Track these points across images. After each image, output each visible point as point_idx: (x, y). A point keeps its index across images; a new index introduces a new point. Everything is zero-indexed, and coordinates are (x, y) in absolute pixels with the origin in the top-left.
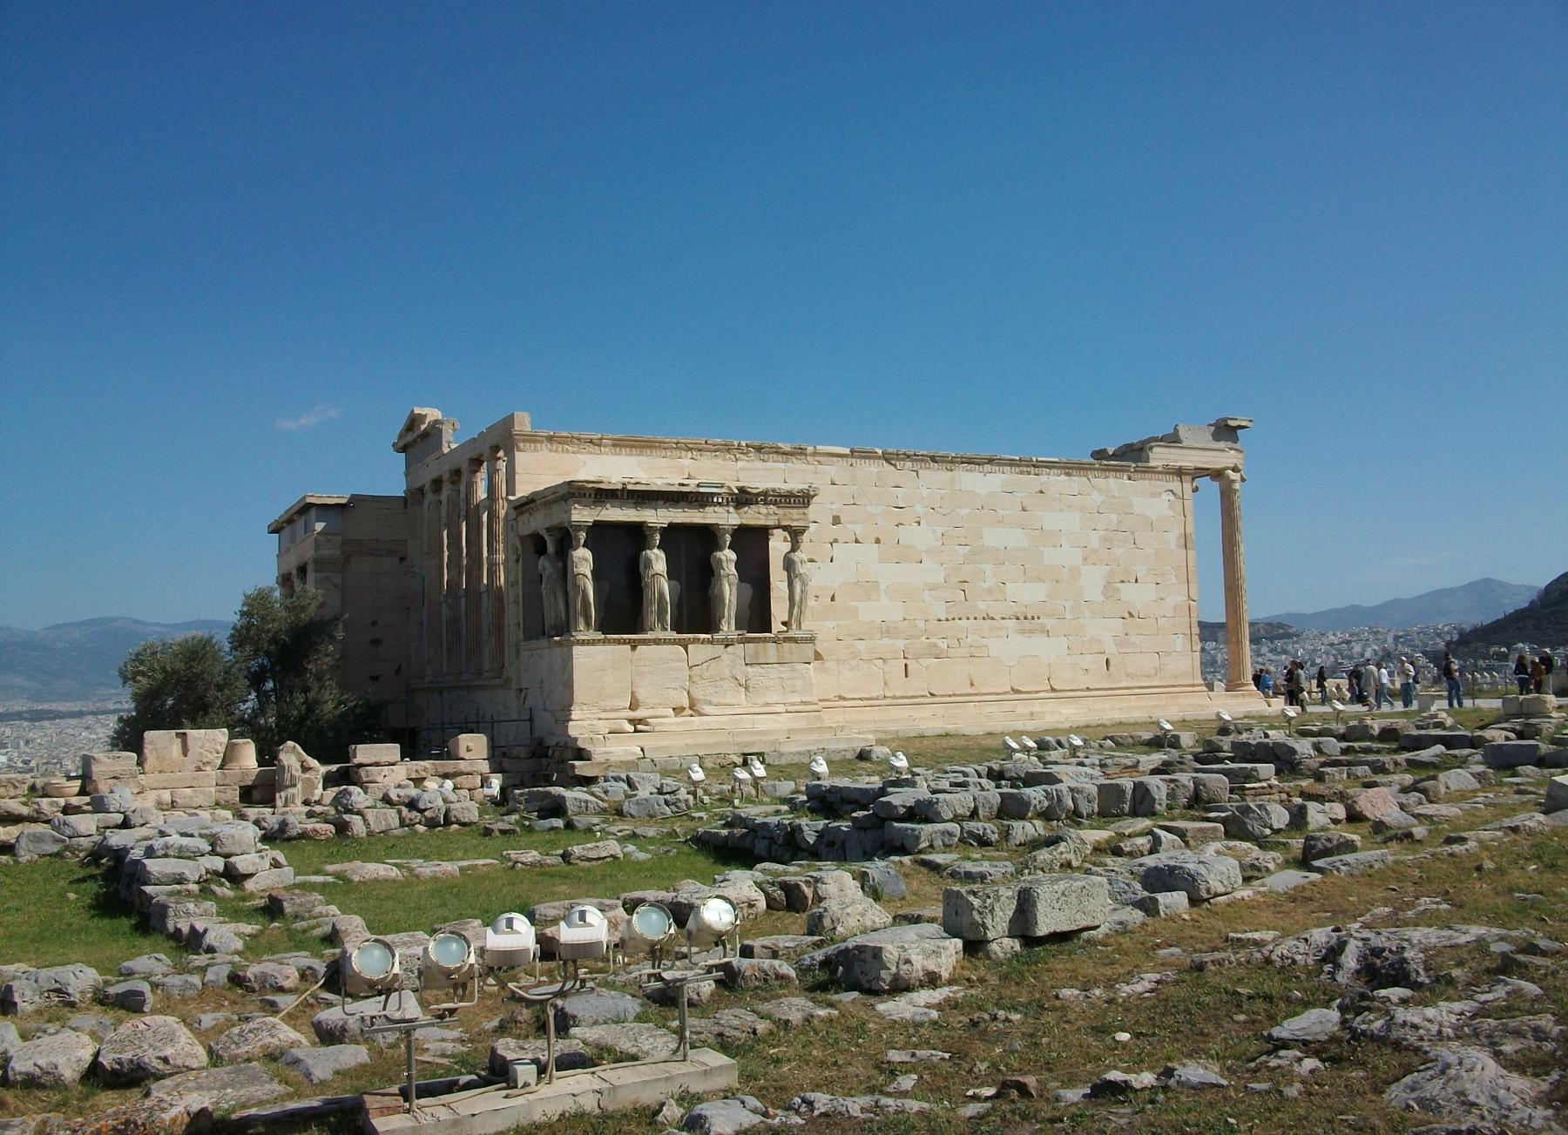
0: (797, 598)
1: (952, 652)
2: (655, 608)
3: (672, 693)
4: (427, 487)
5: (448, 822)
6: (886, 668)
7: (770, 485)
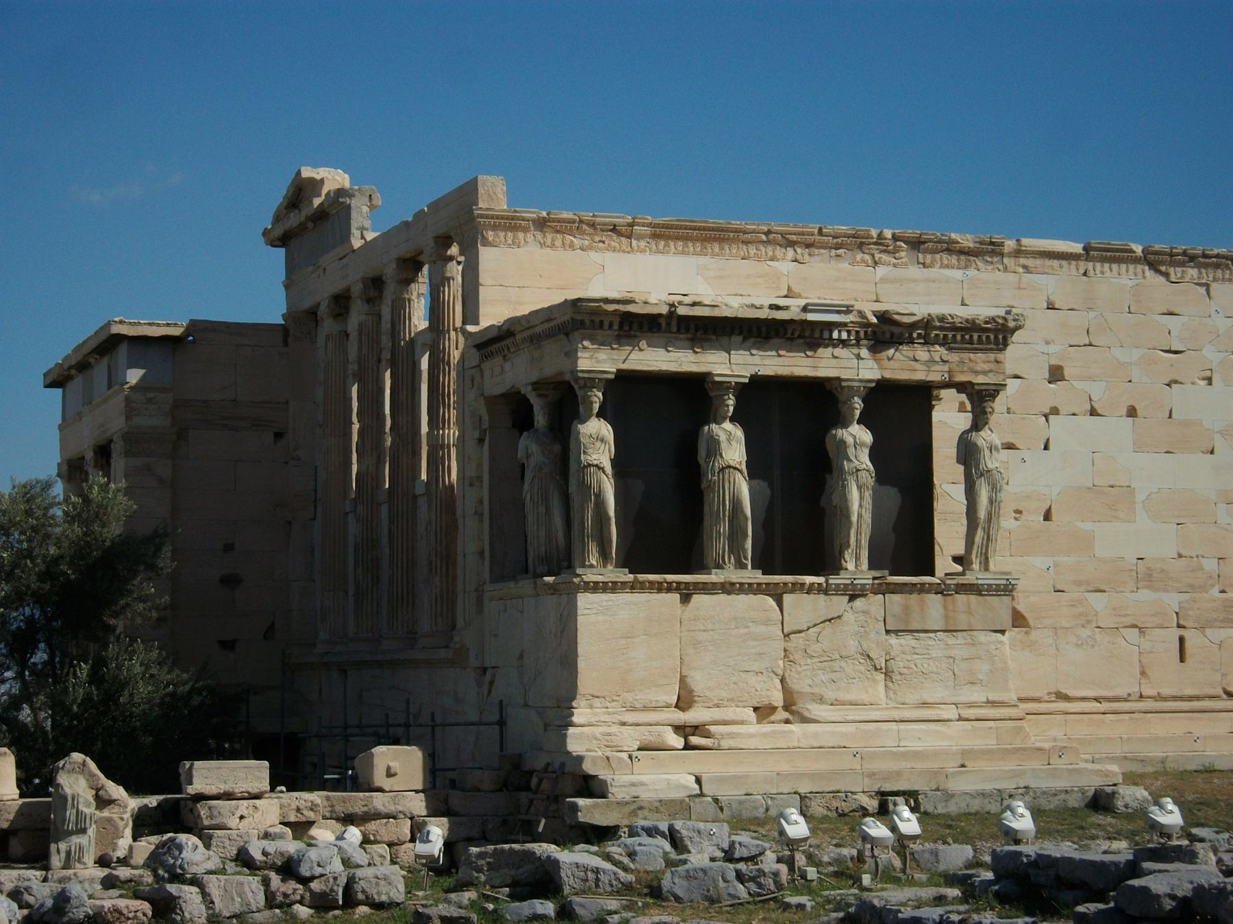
0: (982, 514)
2: (724, 528)
3: (753, 680)
4: (323, 309)
5: (350, 901)
6: (1146, 645)
7: (936, 309)
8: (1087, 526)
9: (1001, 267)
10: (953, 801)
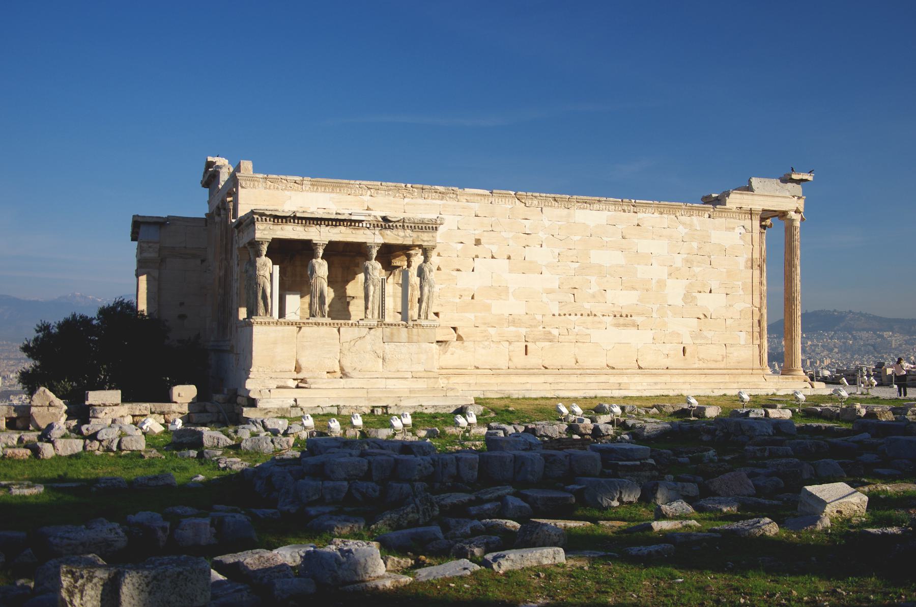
1: (562, 338)
8: (489, 301)
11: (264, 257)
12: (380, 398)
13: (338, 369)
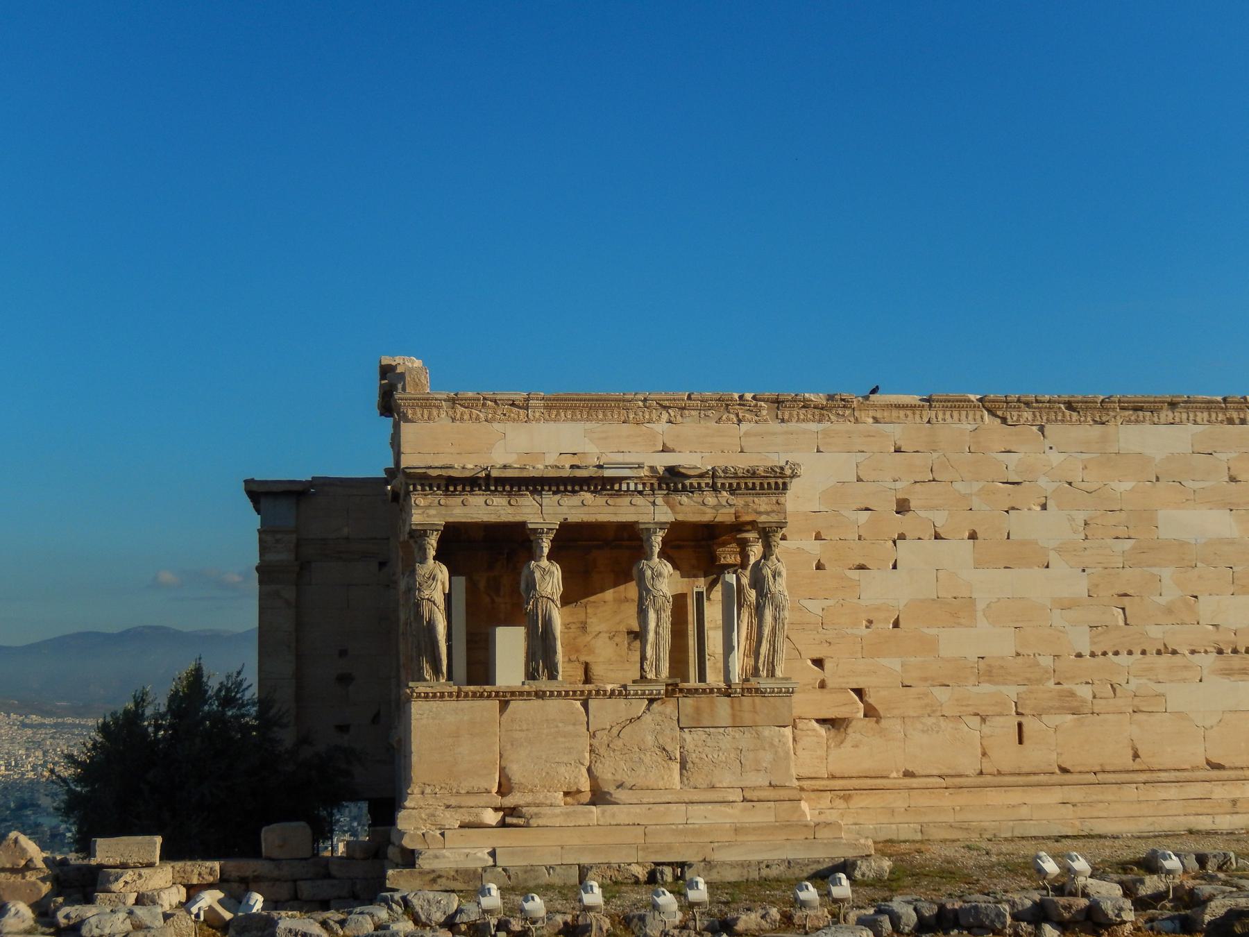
1: (1099, 705)
3: (562, 769)
7: (721, 461)
9: (852, 419)
10: (715, 870)
11: (431, 561)
12: (669, 847)
13: (585, 785)
